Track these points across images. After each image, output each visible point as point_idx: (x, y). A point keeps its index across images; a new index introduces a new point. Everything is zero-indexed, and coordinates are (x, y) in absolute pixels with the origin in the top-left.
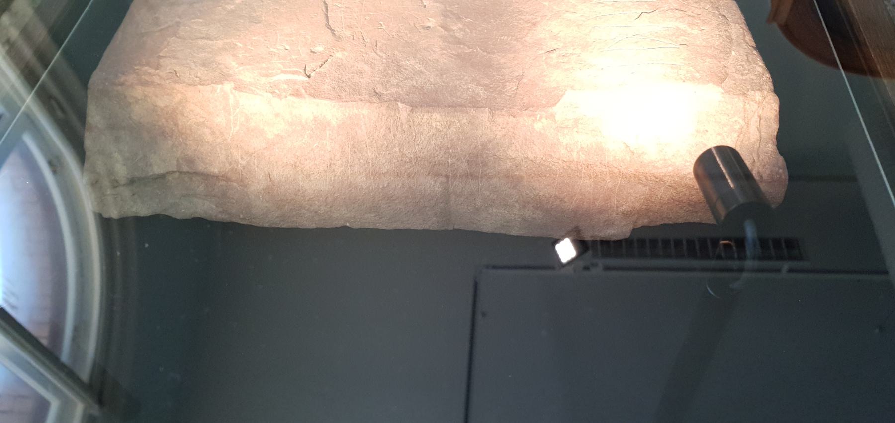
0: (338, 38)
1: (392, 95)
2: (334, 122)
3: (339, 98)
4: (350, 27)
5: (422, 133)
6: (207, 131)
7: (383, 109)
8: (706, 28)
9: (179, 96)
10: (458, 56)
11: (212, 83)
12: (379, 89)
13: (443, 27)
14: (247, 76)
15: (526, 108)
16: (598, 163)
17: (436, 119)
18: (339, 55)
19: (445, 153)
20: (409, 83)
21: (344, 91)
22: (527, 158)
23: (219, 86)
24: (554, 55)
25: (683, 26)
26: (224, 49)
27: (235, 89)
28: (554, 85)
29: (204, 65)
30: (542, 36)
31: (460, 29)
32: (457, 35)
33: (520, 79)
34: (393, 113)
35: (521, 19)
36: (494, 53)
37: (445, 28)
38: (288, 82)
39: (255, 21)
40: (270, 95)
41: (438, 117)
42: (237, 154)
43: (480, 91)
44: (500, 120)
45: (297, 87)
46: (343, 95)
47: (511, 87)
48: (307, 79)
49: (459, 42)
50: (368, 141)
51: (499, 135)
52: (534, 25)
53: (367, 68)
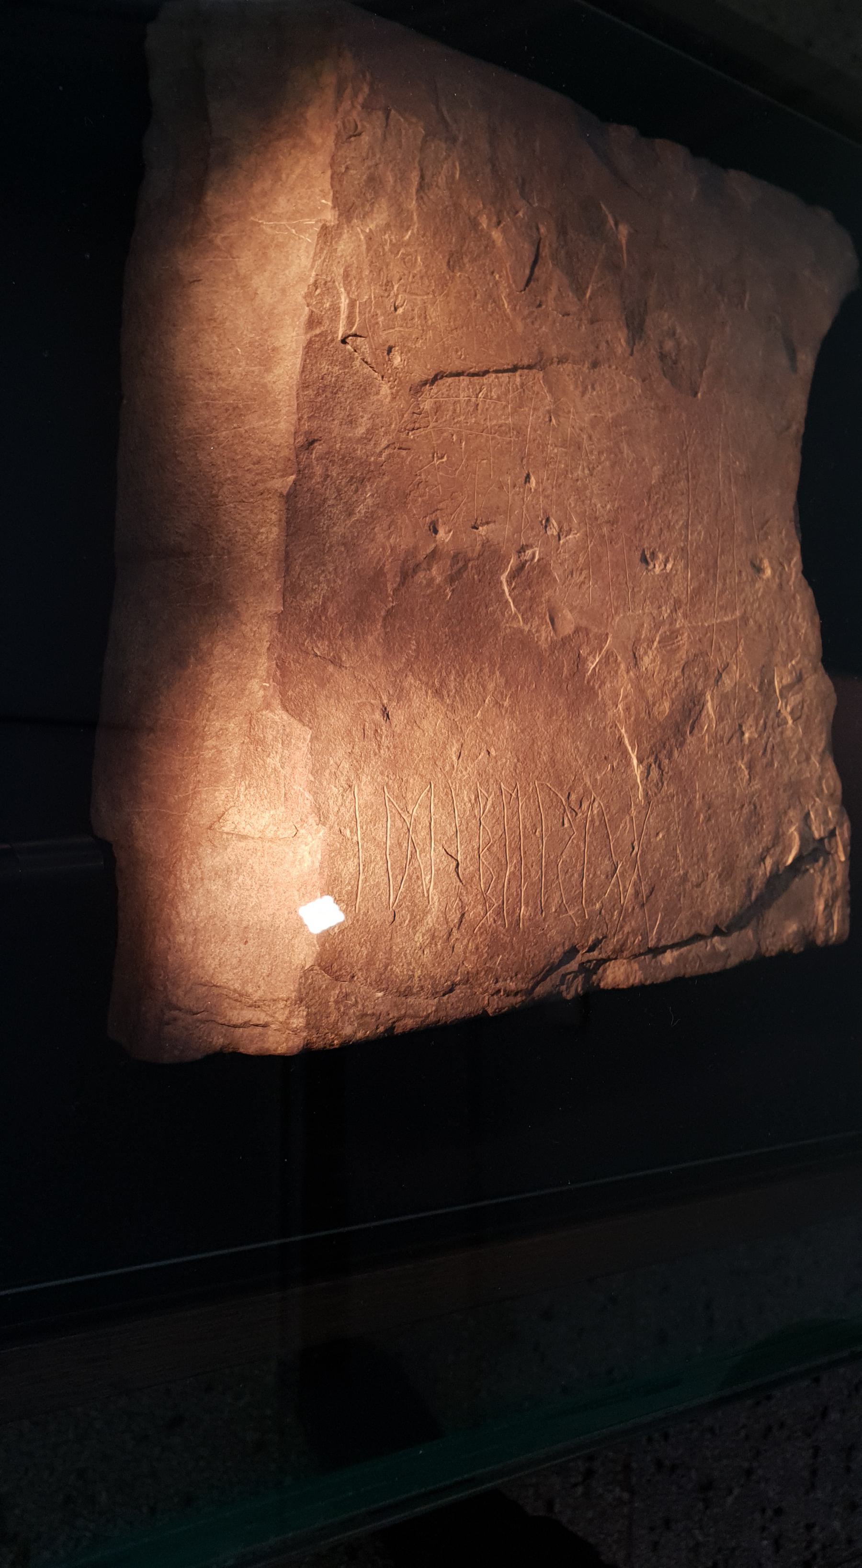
0: (417, 390)
1: (309, 466)
2: (270, 378)
3: (304, 385)
4: (438, 408)
5: (252, 512)
6: (267, 185)
7: (285, 453)
8: (427, 957)
9: (318, 141)
11: (335, 193)
12: (319, 448)
13: (434, 552)
14: (347, 246)
15: (281, 665)
16: (199, 777)
17: (270, 533)
18: (385, 389)
19: (223, 548)
20: (331, 494)
21: (319, 394)
22: (211, 672)
23: (330, 204)
24: (378, 716)
25: (430, 920)
26: (400, 211)
27: (324, 228)
28: (322, 711)
29: (371, 179)
30: (416, 702)
31: (432, 580)
32: (421, 575)
33: (336, 661)
34: (279, 467)
35: (449, 674)
36: (384, 626)
37: (434, 555)
38: (335, 308)
39: (454, 261)
40: (312, 280)
41: (273, 536)
42: (231, 230)
43: (315, 600)
44: (265, 629)
45: (327, 322)
46: (311, 392)
48: (340, 338)
49: (406, 575)
50: (242, 430)
51: (246, 629)
52: (437, 693)
53: (361, 431)
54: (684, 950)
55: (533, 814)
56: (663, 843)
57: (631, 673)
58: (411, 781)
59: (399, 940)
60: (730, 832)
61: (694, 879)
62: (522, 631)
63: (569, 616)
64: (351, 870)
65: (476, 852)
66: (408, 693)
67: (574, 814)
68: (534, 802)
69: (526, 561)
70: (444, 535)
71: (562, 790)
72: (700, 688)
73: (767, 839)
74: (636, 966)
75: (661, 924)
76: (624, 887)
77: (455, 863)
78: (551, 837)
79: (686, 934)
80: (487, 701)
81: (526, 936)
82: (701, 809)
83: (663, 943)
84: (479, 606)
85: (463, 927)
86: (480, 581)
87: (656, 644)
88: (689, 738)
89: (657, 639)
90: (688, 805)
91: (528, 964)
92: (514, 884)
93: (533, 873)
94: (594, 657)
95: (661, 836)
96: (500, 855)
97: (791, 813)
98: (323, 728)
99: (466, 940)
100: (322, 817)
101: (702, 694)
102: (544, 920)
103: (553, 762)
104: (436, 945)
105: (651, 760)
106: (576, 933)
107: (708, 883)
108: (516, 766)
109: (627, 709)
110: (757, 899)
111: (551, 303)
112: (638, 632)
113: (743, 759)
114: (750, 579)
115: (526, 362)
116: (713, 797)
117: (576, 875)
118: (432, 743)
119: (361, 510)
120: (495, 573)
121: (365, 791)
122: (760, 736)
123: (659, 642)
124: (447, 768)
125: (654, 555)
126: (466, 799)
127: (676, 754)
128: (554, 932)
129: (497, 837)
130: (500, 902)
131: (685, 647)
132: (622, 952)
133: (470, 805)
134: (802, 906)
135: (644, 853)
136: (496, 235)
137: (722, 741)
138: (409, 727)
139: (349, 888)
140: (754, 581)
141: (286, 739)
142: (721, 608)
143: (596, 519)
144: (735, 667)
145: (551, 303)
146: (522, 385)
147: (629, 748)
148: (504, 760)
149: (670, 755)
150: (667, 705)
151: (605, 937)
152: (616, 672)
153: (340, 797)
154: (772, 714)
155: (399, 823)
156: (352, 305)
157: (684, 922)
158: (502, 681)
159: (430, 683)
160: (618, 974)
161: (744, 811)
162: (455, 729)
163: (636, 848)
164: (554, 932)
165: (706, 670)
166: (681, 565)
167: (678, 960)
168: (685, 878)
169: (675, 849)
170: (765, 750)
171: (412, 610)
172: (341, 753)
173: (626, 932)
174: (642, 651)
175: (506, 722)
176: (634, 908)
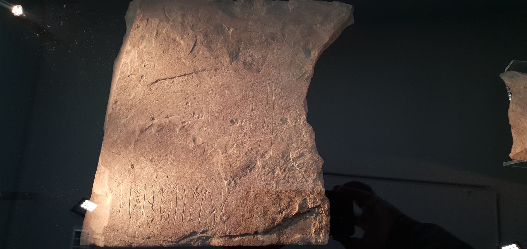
1: (116, 107)
8: (141, 229)
10: (135, 131)
12: (118, 103)
18: (140, 86)
24: (130, 167)
30: (143, 163)
31: (152, 132)
33: (119, 153)
47: (115, 150)
53: (132, 97)
54: (244, 237)
61: (247, 216)
70: (156, 120)
71: (194, 187)
72: (254, 159)
73: (283, 206)
74: (222, 240)
79: (242, 232)
83: (232, 234)
85: (153, 222)
92: (173, 213)
96: (169, 204)
97: (296, 198)
100: (111, 191)
101: (255, 160)
103: (191, 180)
105: (231, 180)
107: (254, 218)
109: (222, 165)
110: (278, 225)
111: (200, 56)
112: (228, 142)
115: (189, 73)
119: (130, 116)
120: (174, 129)
121: (124, 185)
122: (282, 173)
125: (236, 120)
127: (243, 178)
134: (304, 230)
135: (226, 207)
136: (182, 42)
137: (264, 174)
140: (282, 125)
141: (104, 172)
142: (265, 134)
143: (213, 112)
145: (200, 56)
146: (188, 79)
150: (238, 164)
151: (207, 230)
154: (289, 166)
155: (134, 194)
156: (131, 68)
158: (174, 158)
161: (273, 196)
162: (156, 170)
164: (187, 227)
165: (257, 153)
166: (248, 123)
167: (240, 240)
168: (243, 215)
169: (239, 207)
170: (284, 178)
172: (117, 176)
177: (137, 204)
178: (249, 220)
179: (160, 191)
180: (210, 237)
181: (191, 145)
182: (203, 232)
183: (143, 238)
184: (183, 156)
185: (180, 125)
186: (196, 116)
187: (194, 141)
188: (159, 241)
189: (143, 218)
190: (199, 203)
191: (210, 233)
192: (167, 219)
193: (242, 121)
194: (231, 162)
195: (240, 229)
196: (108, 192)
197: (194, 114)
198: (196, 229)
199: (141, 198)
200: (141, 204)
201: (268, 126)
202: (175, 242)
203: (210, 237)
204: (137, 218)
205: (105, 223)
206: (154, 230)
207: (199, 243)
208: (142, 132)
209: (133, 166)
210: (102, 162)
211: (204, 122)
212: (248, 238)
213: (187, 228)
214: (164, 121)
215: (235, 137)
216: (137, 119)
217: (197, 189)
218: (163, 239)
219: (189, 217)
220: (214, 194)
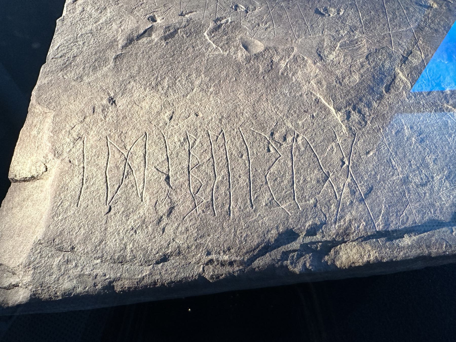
24: (105, 102)
55: (238, 145)
56: (375, 158)
57: (318, 64)
58: (130, 133)
59: (113, 224)
60: (449, 148)
62: (223, 56)
63: (259, 43)
64: (76, 182)
65: (186, 170)
66: (131, 90)
67: (279, 145)
68: (239, 139)
69: (222, 24)
71: (265, 131)
75: (387, 213)
76: (338, 188)
77: (165, 176)
78: (257, 158)
80: (195, 90)
81: (237, 222)
82: (411, 136)
83: (392, 227)
84: (188, 48)
85: (172, 216)
86: (187, 37)
87: (337, 48)
88: (387, 96)
89: (338, 45)
90: (396, 133)
91: (241, 242)
92: (223, 189)
93: (241, 181)
94: (285, 60)
95: (371, 154)
96: (209, 171)
98: (63, 110)
99: (176, 224)
101: (392, 69)
102: (255, 211)
103: (255, 116)
104: (147, 227)
105: (350, 108)
106: (290, 220)
108: (220, 120)
109: (319, 82)
113: (448, 102)
114: (418, 10)
116: (423, 127)
117: (286, 182)
118: (149, 112)
123: (340, 47)
124: (161, 125)
125: (326, 10)
126: (176, 140)
127: (375, 105)
128: (266, 219)
129: (205, 161)
130: (209, 200)
131: (366, 46)
132: (348, 235)
133: (179, 143)
138: (129, 106)
139: (74, 193)
144: (419, 53)
147: (327, 104)
148: (210, 118)
149: (369, 105)
150: (356, 77)
152: (305, 65)
153: (72, 143)
155: (117, 155)
157: (414, 211)
159: (148, 84)
160: (350, 255)
163: (347, 163)
168: (405, 181)
169: (389, 161)
171: (136, 54)
172: (75, 121)
173: (347, 219)
174: (326, 53)
175: (211, 99)
176: (352, 202)
177: (125, 175)
178: (425, 189)
179: (182, 144)
180: (334, 243)
181: (241, 55)
182: (312, 232)
183: (147, 262)
184: (227, 75)
185: (212, 25)
186: (242, 8)
187: (246, 48)
188: (195, 267)
189: (145, 209)
190: (285, 164)
191: (332, 231)
192: (210, 205)
193: (339, 11)
194: (339, 75)
195: (411, 213)
196: (51, 156)
197: (237, 6)
198: (292, 224)
199: (136, 162)
200: (137, 176)
201: (394, 14)
202: (242, 263)
203: (334, 243)
204: (127, 209)
205: (39, 233)
206: (176, 235)
207: (308, 260)
208: (130, 41)
209: (112, 101)
210: (39, 97)
211: (260, 16)
212: (437, 234)
213: (267, 222)
214: (175, 20)
215: (334, 34)
216: (118, 22)
217: (272, 134)
218: (206, 259)
219: (267, 196)
220: (318, 140)
